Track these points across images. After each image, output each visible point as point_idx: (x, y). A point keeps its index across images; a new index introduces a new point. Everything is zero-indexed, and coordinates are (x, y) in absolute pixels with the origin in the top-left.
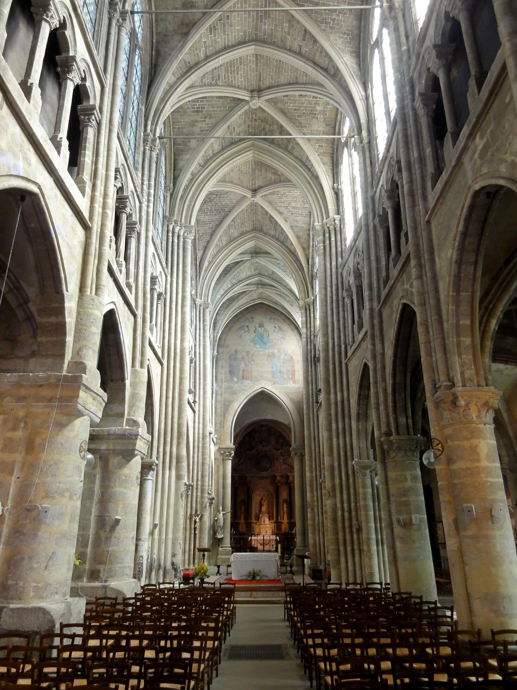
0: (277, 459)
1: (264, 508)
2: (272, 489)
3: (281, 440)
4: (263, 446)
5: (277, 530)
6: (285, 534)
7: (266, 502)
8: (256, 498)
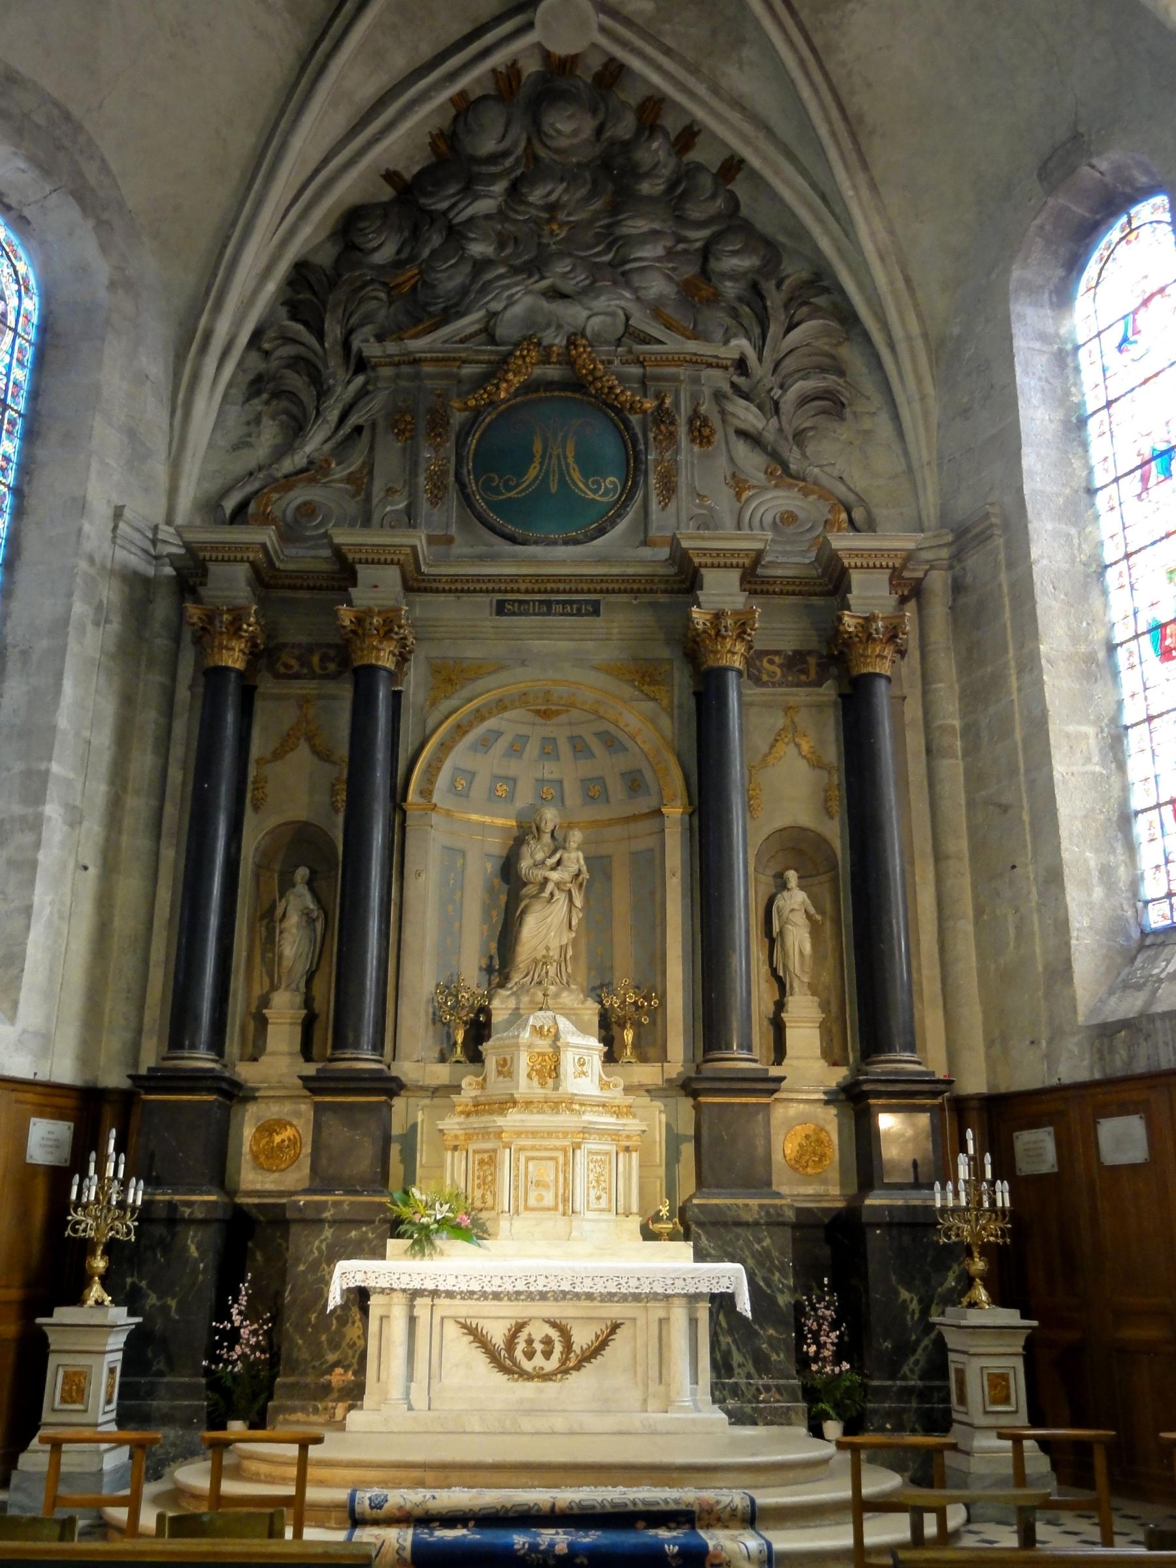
0: (700, 431)
1: (546, 929)
2: (648, 727)
3: (735, 262)
4: (556, 294)
7: (575, 859)
8: (459, 816)
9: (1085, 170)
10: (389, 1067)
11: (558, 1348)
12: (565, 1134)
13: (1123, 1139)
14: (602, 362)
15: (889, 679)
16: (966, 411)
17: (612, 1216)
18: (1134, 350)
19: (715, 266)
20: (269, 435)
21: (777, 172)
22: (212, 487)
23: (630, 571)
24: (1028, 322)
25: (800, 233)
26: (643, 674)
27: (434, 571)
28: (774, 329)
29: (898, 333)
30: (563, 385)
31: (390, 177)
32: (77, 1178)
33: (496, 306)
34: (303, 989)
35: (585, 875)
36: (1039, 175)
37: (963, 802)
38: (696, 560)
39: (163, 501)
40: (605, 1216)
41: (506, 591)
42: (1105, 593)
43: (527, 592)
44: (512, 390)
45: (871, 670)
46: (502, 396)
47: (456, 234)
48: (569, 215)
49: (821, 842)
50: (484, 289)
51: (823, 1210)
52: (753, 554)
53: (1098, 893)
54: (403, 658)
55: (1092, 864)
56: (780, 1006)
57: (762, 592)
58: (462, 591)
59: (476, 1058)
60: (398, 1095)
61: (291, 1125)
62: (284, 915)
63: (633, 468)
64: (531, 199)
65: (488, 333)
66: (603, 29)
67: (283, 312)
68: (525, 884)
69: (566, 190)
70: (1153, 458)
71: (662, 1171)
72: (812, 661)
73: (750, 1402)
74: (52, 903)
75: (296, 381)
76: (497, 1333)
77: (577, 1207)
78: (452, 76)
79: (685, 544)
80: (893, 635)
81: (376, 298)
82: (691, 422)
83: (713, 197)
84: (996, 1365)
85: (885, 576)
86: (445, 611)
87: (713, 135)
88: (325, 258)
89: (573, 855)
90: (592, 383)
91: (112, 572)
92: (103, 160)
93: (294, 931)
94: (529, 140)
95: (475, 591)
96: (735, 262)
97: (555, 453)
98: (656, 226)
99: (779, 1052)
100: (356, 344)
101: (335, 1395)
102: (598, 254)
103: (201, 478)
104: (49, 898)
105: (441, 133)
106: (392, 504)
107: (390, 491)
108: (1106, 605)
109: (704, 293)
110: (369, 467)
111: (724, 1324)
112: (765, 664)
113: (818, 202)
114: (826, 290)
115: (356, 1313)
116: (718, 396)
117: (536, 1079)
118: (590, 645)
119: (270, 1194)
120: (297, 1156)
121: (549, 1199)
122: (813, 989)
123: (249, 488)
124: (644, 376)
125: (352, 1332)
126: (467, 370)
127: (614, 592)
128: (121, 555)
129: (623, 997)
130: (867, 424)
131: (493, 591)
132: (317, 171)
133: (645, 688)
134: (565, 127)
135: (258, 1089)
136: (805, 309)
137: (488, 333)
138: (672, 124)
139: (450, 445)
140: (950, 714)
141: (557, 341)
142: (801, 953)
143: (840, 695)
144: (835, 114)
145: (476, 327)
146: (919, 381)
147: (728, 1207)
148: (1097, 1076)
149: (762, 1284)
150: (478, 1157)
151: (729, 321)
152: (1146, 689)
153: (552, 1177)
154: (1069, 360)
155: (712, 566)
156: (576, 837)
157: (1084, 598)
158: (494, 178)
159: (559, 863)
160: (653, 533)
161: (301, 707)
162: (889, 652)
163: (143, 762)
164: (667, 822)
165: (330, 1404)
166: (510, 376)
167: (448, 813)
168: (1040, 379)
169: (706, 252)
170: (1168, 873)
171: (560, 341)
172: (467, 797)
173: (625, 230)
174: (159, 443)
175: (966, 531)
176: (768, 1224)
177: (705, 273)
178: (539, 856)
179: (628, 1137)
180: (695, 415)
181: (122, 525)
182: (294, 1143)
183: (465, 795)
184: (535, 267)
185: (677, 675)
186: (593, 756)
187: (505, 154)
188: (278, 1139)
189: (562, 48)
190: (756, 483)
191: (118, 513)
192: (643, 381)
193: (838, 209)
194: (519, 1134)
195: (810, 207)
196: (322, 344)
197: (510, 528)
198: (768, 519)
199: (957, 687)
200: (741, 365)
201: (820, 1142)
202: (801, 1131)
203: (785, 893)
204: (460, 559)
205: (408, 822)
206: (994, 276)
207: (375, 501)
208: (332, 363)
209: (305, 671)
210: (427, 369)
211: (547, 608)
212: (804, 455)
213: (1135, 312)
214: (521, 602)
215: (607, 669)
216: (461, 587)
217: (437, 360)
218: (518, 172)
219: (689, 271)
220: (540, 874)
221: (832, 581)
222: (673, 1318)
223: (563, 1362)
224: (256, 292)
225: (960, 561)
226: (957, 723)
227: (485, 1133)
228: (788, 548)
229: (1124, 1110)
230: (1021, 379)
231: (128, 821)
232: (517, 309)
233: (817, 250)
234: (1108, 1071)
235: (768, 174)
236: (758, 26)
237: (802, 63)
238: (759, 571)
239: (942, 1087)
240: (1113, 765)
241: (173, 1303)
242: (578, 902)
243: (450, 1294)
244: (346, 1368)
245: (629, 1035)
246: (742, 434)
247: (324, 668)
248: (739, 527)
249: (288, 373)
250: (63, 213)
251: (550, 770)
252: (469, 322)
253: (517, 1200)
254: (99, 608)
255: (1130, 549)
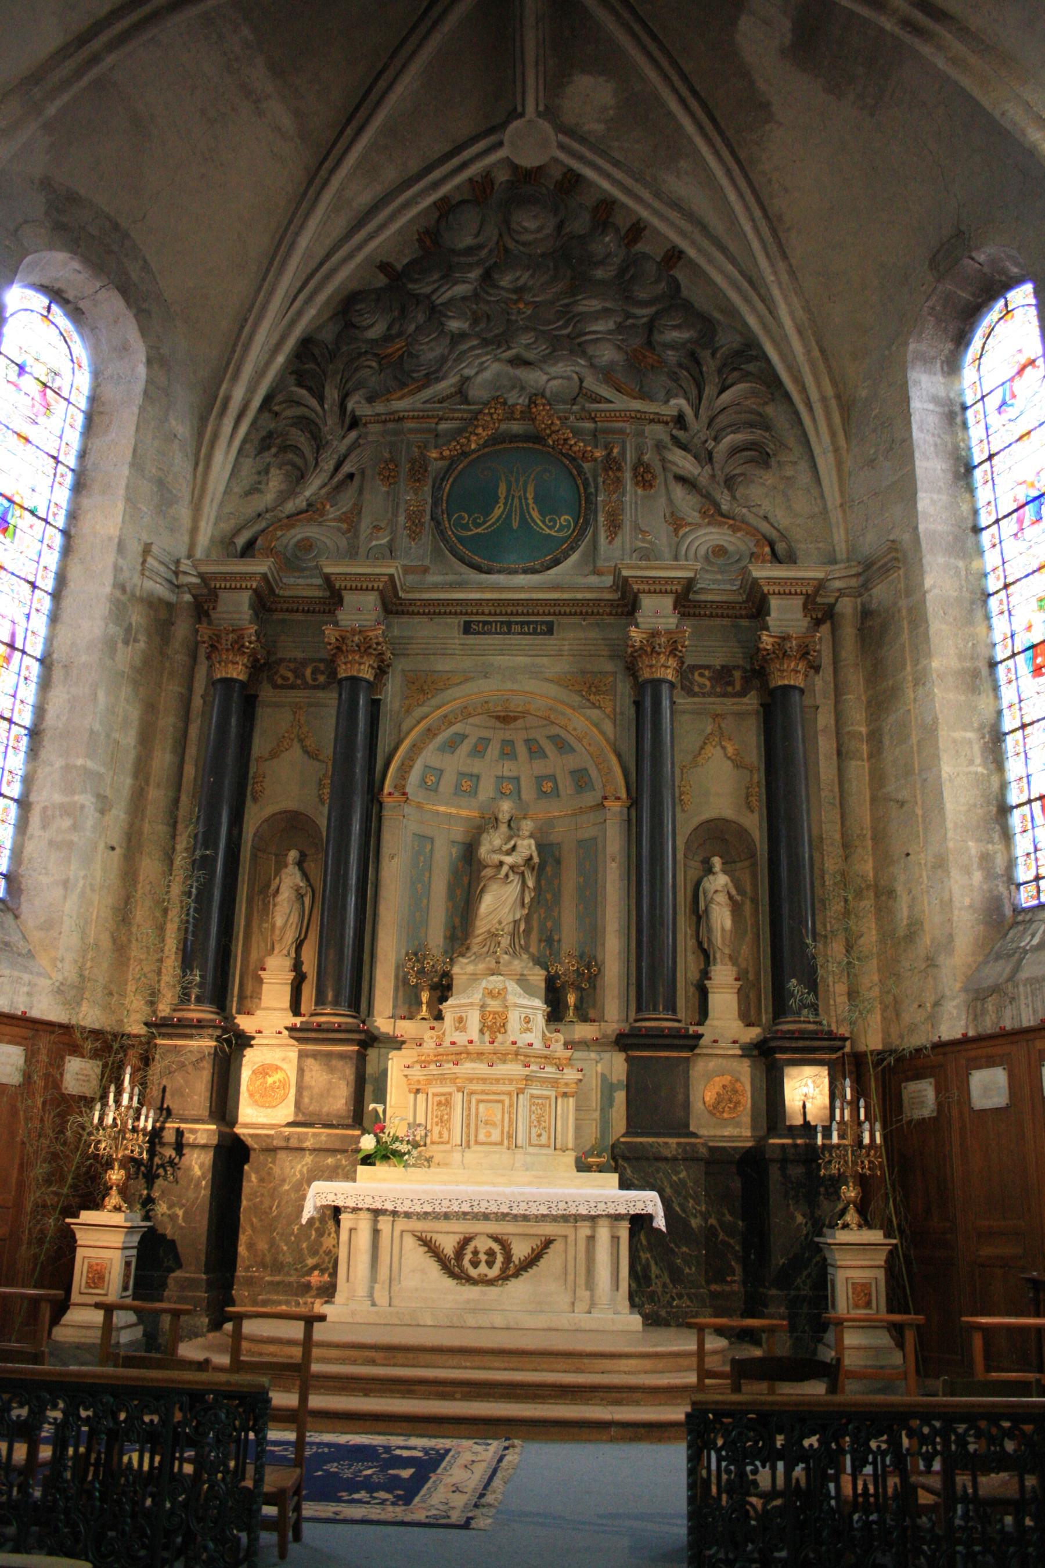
1: (499, 904)
2: (594, 731)
5: (634, 1124)
6: (717, 1161)
7: (527, 847)
9: (967, 261)
10: (364, 1022)
11: (500, 1259)
12: (511, 1081)
13: (989, 1087)
14: (559, 418)
15: (802, 691)
16: (873, 461)
17: (551, 1151)
18: (1011, 412)
19: (657, 337)
20: (275, 483)
21: (711, 261)
22: (226, 527)
23: (579, 596)
24: (924, 388)
25: (732, 312)
26: (587, 686)
27: (410, 596)
28: (709, 390)
29: (814, 395)
30: (527, 438)
31: (384, 267)
32: (98, 1106)
33: (468, 372)
34: (293, 955)
35: (536, 860)
36: (930, 265)
37: (868, 798)
38: (635, 587)
39: (186, 538)
40: (544, 1151)
41: (472, 613)
42: (988, 617)
43: (490, 614)
44: (481, 442)
45: (786, 682)
46: (473, 446)
47: (436, 313)
48: (534, 296)
49: (742, 832)
50: (458, 360)
51: (735, 1148)
52: (684, 582)
53: (978, 876)
54: (381, 671)
55: (973, 851)
56: (705, 974)
57: (694, 615)
58: (434, 613)
59: (439, 1017)
60: (372, 1046)
61: (282, 1069)
62: (278, 890)
63: (585, 512)
64: (502, 284)
65: (461, 393)
66: (561, 147)
67: (292, 380)
68: (485, 867)
69: (532, 276)
70: (1027, 503)
71: (597, 1115)
72: (737, 674)
73: (664, 1307)
74: (85, 877)
75: (301, 439)
76: (448, 1245)
77: (519, 1143)
78: (436, 185)
79: (625, 573)
80: (804, 653)
81: (370, 367)
82: (635, 469)
83: (658, 281)
84: (857, 1275)
85: (798, 602)
86: (422, 631)
87: (656, 231)
88: (328, 335)
89: (526, 842)
90: (549, 436)
91: (141, 600)
92: (145, 261)
93: (285, 904)
94: (500, 235)
95: (445, 613)
96: (675, 334)
97: (517, 495)
98: (608, 305)
99: (703, 1012)
100: (350, 406)
101: (314, 1292)
102: (559, 328)
103: (218, 518)
104: (82, 873)
105: (427, 232)
106: (377, 539)
107: (378, 528)
108: (990, 627)
109: (650, 361)
110: (357, 510)
111: (644, 1242)
112: (696, 677)
113: (746, 285)
114: (756, 358)
115: (331, 1223)
116: (659, 446)
117: (487, 1034)
118: (545, 660)
119: (263, 1126)
120: (286, 1096)
121: (496, 1136)
122: (733, 959)
123: (257, 528)
124: (596, 429)
125: (328, 1242)
126: (443, 426)
127: (565, 614)
128: (149, 584)
129: (566, 966)
130: (789, 472)
131: (461, 613)
132: (321, 264)
133: (592, 697)
134: (531, 224)
135: (253, 1038)
136: (736, 374)
137: (461, 393)
138: (623, 222)
139: (427, 489)
140: (858, 723)
141: (520, 401)
142: (723, 929)
143: (762, 705)
144: (758, 213)
145: (453, 390)
146: (833, 435)
147: (651, 1145)
148: (971, 1033)
149: (678, 1209)
150: (437, 1099)
151: (670, 384)
152: (1020, 701)
153: (499, 1117)
154: (959, 420)
155: (649, 592)
156: (527, 826)
157: (970, 622)
158: (470, 266)
159: (514, 848)
160: (600, 564)
161: (295, 713)
162: (801, 666)
163: (162, 759)
164: (609, 815)
165: (310, 1300)
166: (480, 430)
167: (419, 806)
168: (933, 435)
169: (651, 327)
170: (1036, 859)
171: (523, 400)
172: (436, 790)
173: (581, 309)
174: (183, 490)
175: (873, 564)
176: (684, 1159)
177: (649, 344)
178: (497, 842)
179: (566, 1084)
180: (639, 463)
181: (150, 560)
182: (284, 1084)
183: (435, 789)
184: (502, 341)
185: (620, 685)
186: (545, 756)
187: (480, 247)
188: (270, 1080)
189: (528, 160)
190: (690, 520)
191: (147, 550)
192: (595, 434)
193: (763, 291)
194: (471, 1080)
195: (738, 289)
196: (322, 406)
197: (477, 559)
198: (702, 551)
199: (863, 698)
200: (680, 420)
201: (735, 1091)
202: (718, 1082)
203: (711, 877)
204: (436, 587)
205: (385, 813)
206: (894, 348)
207: (363, 536)
208: (329, 422)
209: (299, 682)
210: (409, 425)
211: (508, 628)
212: (734, 498)
213: (1012, 379)
214: (485, 623)
215: (557, 682)
216: (435, 610)
217: (418, 417)
218: (492, 262)
219: (637, 342)
220: (496, 858)
221: (755, 605)
222: (597, 1236)
223: (504, 1270)
224: (268, 364)
225: (868, 590)
226: (863, 730)
227: (442, 1079)
228: (719, 577)
229: (990, 1062)
230: (916, 434)
231: (150, 811)
232: (487, 375)
233: (745, 324)
234: (980, 1030)
235: (701, 261)
236: (691, 142)
237: (728, 172)
238: (691, 596)
239: (839, 1043)
240: (992, 766)
241: (180, 1213)
242: (531, 884)
243: (408, 1215)
244: (323, 1271)
245: (571, 999)
246: (681, 479)
247: (315, 680)
248: (676, 558)
249: (294, 430)
250: (113, 303)
251: (508, 769)
252: (445, 386)
253: (468, 1136)
254: (128, 630)
255: (1009, 580)
